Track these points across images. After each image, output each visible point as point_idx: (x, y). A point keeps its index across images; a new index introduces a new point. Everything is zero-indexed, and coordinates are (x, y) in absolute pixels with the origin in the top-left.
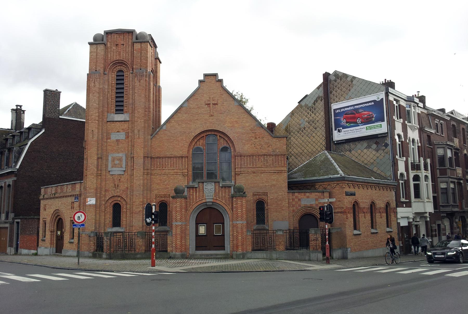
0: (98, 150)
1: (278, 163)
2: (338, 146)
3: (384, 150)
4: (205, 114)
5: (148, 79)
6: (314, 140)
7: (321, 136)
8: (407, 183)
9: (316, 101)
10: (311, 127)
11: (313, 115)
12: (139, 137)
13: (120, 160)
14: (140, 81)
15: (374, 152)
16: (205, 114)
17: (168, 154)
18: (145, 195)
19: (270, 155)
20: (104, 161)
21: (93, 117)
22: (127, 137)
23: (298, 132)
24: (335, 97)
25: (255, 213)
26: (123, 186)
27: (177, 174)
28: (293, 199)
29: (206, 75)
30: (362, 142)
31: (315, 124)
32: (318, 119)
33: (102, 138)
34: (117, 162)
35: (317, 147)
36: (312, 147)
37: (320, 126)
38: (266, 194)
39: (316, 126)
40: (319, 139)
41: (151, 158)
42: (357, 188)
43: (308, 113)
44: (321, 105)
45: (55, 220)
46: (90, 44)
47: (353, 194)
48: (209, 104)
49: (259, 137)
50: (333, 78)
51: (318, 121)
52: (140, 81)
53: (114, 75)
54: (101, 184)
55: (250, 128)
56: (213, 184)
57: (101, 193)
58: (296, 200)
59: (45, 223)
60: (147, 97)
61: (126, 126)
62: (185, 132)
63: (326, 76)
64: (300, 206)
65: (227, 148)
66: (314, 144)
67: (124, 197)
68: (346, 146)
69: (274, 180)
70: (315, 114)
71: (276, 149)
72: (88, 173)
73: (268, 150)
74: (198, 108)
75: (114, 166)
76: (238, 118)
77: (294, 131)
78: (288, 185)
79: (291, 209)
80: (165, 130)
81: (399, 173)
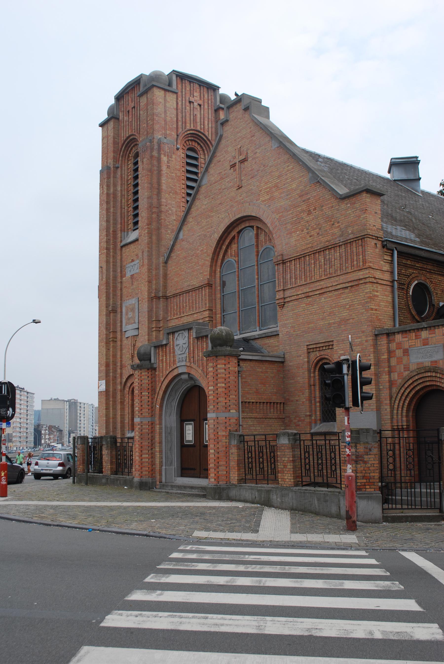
1: (352, 261)
5: (155, 154)
19: (334, 246)
20: (119, 316)
25: (318, 394)
33: (115, 278)
34: (130, 315)
41: (166, 298)
54: (114, 356)
55: (298, 192)
57: (115, 371)
58: (399, 353)
60: (155, 185)
64: (407, 368)
73: (333, 234)
80: (183, 240)
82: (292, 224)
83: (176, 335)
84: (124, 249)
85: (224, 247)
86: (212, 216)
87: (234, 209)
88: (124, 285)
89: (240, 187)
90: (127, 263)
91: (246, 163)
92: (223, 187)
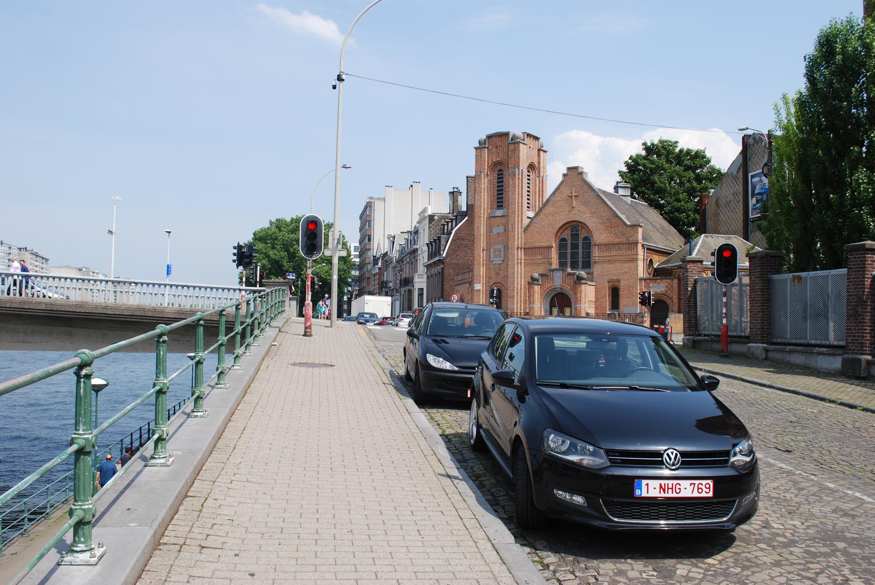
13: (500, 251)
17: (537, 245)
22: (505, 230)
26: (502, 274)
29: (569, 169)
34: (497, 253)
38: (619, 281)
46: (476, 148)
50: (751, 141)
53: (496, 175)
61: (504, 220)
63: (745, 139)
75: (496, 256)
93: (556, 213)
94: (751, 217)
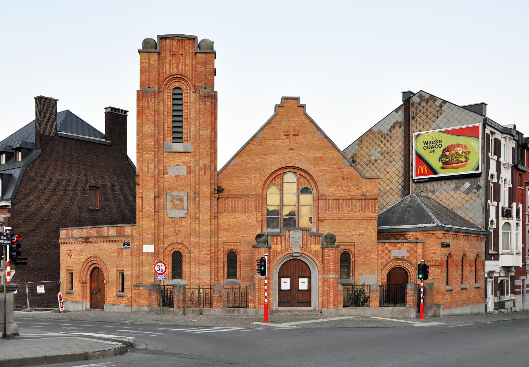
0: (154, 188)
1: (368, 208)
2: (418, 185)
3: (475, 193)
4: (283, 147)
6: (388, 176)
7: (397, 172)
8: (496, 231)
9: (393, 127)
10: (385, 160)
11: (388, 145)
12: (205, 172)
14: (205, 104)
15: (463, 195)
16: (283, 147)
18: (213, 243)
21: (148, 146)
22: (189, 172)
23: (367, 165)
24: (418, 125)
27: (249, 218)
28: (383, 251)
30: (448, 182)
31: (391, 156)
32: (394, 150)
34: (177, 202)
35: (391, 185)
36: (385, 185)
37: (397, 159)
39: (391, 159)
40: (394, 175)
42: (452, 239)
43: (382, 142)
44: (399, 132)
45: (89, 269)
47: (448, 246)
48: (289, 135)
49: (347, 178)
51: (394, 153)
52: (205, 104)
55: (337, 166)
56: (301, 232)
59: (72, 274)
61: (186, 158)
62: (259, 169)
64: (389, 258)
65: (308, 189)
66: (388, 182)
67: (186, 244)
68: (429, 186)
69: (363, 228)
70: (391, 144)
71: (366, 192)
72: (144, 215)
74: (275, 139)
75: (174, 207)
76: (323, 154)
77: (361, 163)
78: (378, 233)
79: (380, 261)
81: (490, 220)
82: (331, 181)
83: (291, 232)
84: (165, 154)
85: (271, 179)
86: (266, 159)
87: (286, 160)
88: (166, 180)
89: (292, 149)
90: (169, 166)
91: (297, 137)
92: (277, 144)
93: (266, 155)
94: (415, 177)
